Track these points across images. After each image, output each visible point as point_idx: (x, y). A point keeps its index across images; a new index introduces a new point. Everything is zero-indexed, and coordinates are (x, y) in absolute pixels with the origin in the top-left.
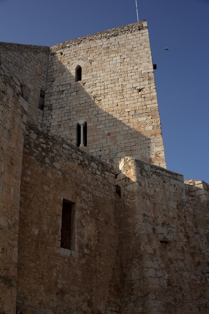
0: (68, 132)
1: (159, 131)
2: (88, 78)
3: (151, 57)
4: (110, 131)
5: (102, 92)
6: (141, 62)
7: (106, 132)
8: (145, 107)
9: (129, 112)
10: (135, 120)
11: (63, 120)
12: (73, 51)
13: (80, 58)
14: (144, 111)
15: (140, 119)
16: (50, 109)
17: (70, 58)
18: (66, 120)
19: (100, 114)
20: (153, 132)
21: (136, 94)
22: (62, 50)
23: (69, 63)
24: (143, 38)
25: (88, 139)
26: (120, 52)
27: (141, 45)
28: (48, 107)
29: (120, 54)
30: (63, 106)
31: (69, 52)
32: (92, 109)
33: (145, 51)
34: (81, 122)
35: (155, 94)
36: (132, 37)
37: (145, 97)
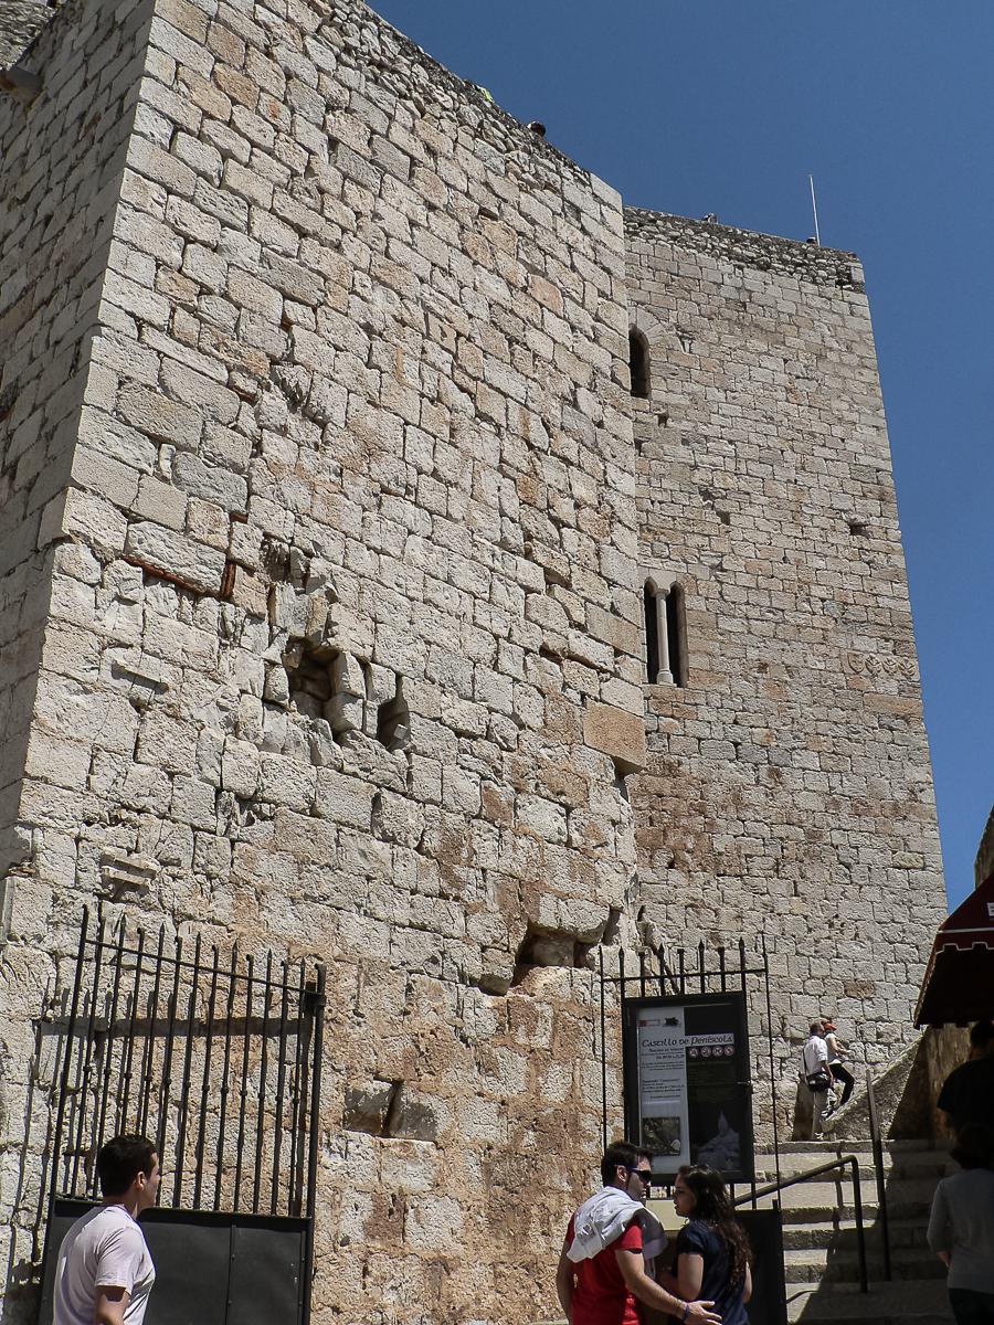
1: (915, 705)
2: (674, 399)
3: (882, 412)
4: (767, 657)
5: (731, 482)
6: (854, 417)
7: (753, 654)
8: (871, 602)
9: (823, 600)
13: (642, 299)
14: (872, 617)
15: (862, 644)
19: (726, 571)
20: (902, 705)
21: (842, 538)
24: (854, 323)
25: (694, 662)
26: (784, 343)
29: (782, 351)
32: (699, 540)
33: (862, 378)
34: (664, 583)
35: (899, 561)
36: (818, 302)
37: (872, 562)
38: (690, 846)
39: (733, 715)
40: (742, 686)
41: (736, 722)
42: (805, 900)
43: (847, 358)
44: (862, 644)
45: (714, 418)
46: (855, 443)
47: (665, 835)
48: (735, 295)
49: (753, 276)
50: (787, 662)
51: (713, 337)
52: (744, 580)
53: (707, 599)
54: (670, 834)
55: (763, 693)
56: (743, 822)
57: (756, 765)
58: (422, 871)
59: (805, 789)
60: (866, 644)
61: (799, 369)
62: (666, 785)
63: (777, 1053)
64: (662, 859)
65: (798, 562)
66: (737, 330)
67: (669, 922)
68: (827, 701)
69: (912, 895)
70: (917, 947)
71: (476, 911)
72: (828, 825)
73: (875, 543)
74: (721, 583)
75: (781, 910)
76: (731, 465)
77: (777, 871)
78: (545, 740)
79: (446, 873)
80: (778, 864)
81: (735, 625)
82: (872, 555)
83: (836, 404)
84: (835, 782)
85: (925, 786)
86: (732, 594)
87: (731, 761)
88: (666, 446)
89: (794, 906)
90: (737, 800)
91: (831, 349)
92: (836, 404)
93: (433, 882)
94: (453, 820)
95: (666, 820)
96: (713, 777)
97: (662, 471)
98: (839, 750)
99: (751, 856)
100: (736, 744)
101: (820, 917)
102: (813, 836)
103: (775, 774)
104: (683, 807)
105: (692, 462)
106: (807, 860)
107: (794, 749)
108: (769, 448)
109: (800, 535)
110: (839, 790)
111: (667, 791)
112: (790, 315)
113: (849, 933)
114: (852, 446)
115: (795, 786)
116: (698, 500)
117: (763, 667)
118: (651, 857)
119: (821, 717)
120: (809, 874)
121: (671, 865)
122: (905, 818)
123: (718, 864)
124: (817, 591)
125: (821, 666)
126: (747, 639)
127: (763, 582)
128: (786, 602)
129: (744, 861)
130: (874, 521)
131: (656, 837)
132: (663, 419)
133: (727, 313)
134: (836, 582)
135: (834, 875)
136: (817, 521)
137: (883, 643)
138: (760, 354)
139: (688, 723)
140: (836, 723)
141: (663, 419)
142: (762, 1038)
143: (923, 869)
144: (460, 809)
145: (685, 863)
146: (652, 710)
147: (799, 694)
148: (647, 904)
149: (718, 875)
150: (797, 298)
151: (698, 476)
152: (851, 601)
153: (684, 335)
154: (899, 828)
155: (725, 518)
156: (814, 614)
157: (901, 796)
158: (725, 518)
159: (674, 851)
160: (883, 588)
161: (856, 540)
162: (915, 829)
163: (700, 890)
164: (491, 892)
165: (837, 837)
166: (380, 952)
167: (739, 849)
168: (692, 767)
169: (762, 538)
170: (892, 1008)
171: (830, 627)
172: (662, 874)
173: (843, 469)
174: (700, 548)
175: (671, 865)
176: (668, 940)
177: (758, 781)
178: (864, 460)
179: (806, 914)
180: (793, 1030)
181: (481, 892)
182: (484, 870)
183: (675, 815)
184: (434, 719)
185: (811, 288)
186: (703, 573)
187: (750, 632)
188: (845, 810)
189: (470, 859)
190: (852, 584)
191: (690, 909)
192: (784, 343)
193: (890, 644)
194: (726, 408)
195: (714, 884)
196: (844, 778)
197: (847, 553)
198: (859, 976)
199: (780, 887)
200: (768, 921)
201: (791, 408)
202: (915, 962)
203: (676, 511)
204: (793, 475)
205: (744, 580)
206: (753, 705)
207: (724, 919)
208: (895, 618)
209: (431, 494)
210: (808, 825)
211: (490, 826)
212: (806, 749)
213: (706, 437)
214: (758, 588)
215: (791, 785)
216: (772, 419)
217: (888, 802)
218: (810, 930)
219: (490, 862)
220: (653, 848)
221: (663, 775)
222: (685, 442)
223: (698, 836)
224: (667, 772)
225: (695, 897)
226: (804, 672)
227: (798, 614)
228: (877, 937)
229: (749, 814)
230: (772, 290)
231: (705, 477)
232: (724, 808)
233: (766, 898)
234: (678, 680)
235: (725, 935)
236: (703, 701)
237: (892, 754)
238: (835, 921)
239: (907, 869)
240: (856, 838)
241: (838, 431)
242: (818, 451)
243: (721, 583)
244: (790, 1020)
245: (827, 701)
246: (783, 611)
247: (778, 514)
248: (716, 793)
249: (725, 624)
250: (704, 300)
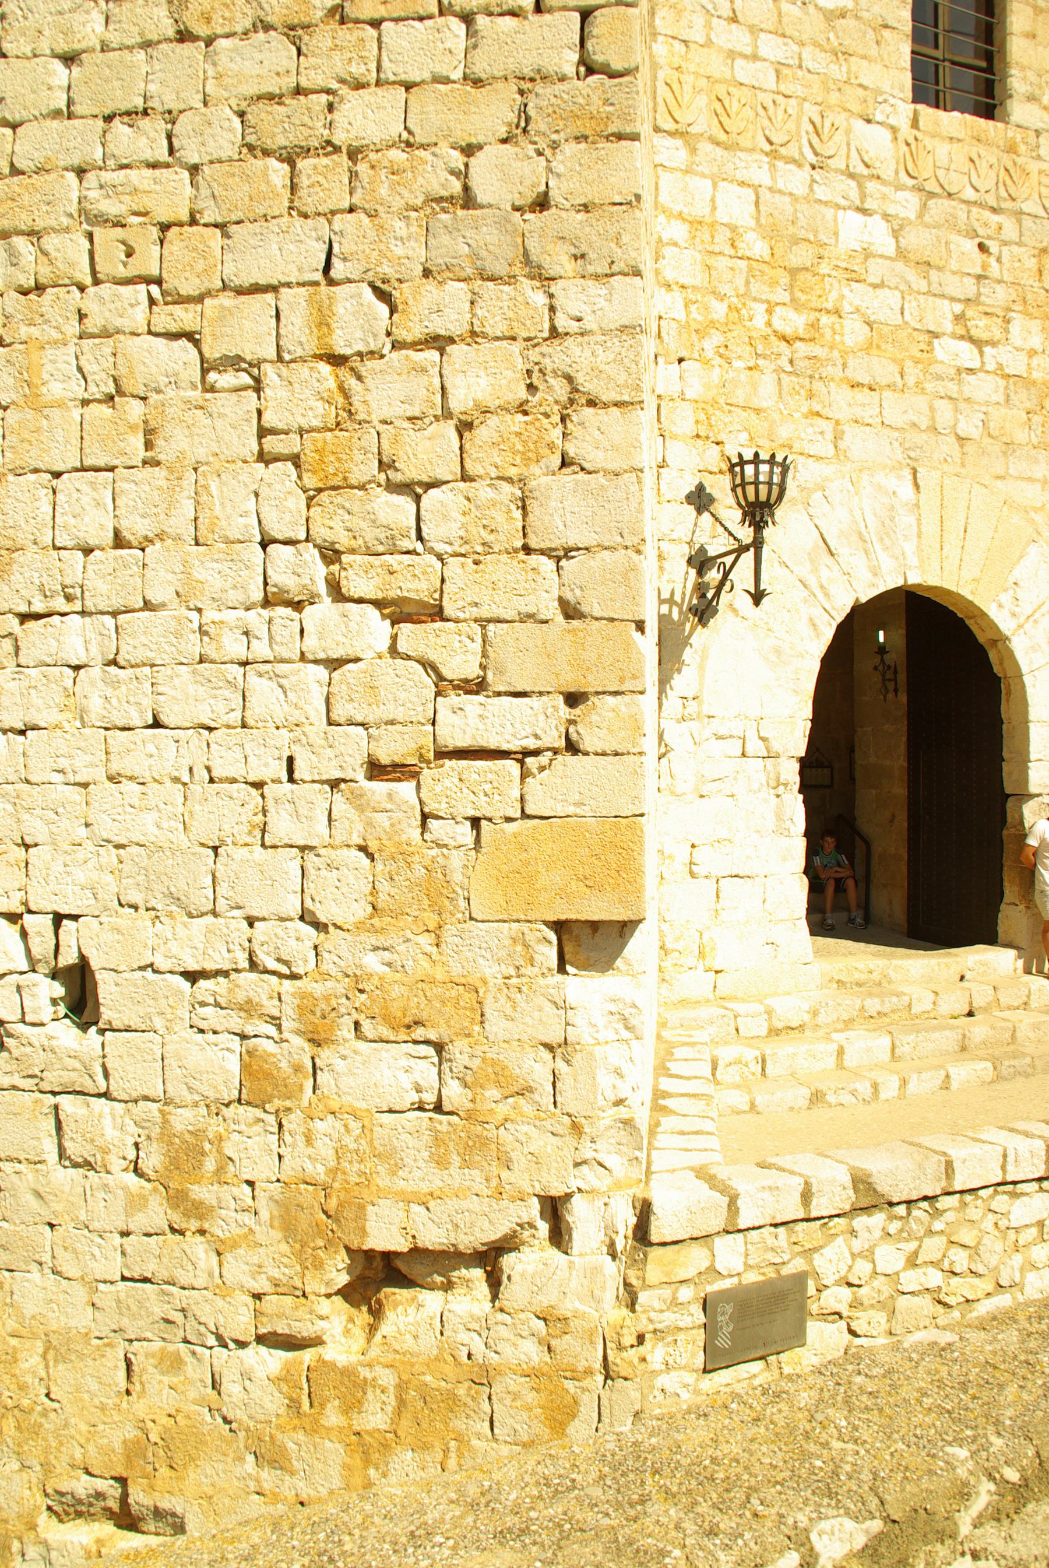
58: (135, 1203)
71: (235, 1245)
78: (373, 940)
79: (177, 1199)
93: (157, 1213)
94: (183, 1120)
144: (197, 1098)
164: (264, 1215)
166: (82, 1319)
181: (248, 1219)
182: (251, 1183)
184: (142, 968)
189: (220, 1170)
209: (105, 579)
211: (259, 1113)
219: (263, 1169)
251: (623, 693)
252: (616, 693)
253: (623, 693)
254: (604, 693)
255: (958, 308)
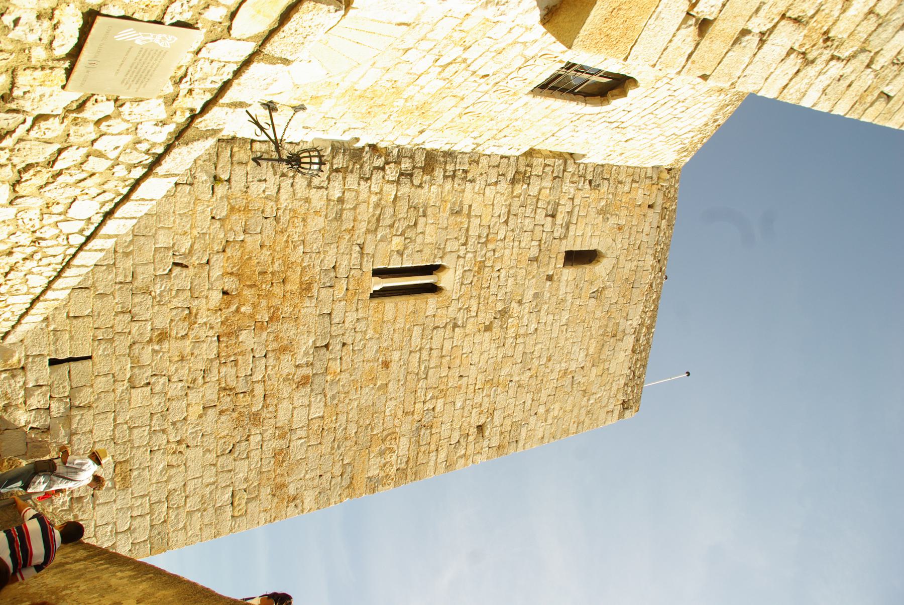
0: (428, 240)
4: (394, 367)
5: (511, 332)
6: (550, 421)
7: (396, 356)
8: (433, 447)
10: (406, 428)
11: (469, 222)
12: (645, 239)
14: (423, 449)
15: (404, 441)
16: (517, 177)
17: (630, 234)
18: (467, 230)
19: (453, 331)
21: (475, 420)
22: (658, 209)
23: (620, 228)
25: (389, 304)
26: (593, 365)
27: (588, 412)
28: (525, 172)
29: (589, 365)
30: (511, 217)
31: (647, 229)
32: (474, 308)
34: (444, 280)
36: (615, 387)
38: (243, 309)
39: (349, 341)
40: (372, 346)
41: (344, 344)
42: (200, 416)
43: (583, 411)
44: (404, 441)
45: (551, 317)
46: (534, 422)
47: (251, 286)
48: (621, 328)
49: (630, 341)
50: (390, 385)
51: (598, 314)
52: (448, 345)
53: (434, 316)
54: (253, 291)
55: (367, 366)
56: (265, 356)
57: (312, 364)
59: (294, 408)
60: (403, 446)
61: (579, 378)
62: (293, 286)
63: (54, 405)
64: (230, 284)
65: (460, 387)
66: (601, 332)
67: (174, 293)
68: (362, 419)
69: (211, 511)
70: (165, 521)
72: (266, 430)
73: (471, 447)
74: (444, 327)
75: (191, 396)
76: (522, 331)
77: (225, 389)
80: (231, 389)
81: (416, 341)
82: (464, 444)
83: (557, 406)
84: (300, 433)
85: (300, 508)
86: (438, 335)
87: (314, 342)
88: (534, 281)
89: (196, 407)
90: (284, 349)
91: (589, 400)
92: (557, 406)
95: (264, 286)
96: (301, 327)
97: (519, 278)
98: (325, 433)
99: (236, 365)
100: (327, 346)
101: (187, 431)
102: (256, 419)
103: (305, 381)
104: (276, 302)
105: (524, 301)
106: (235, 415)
107: (325, 396)
108: (532, 359)
109: (477, 387)
110: (294, 437)
111: (288, 287)
112: (608, 369)
113: (174, 459)
114: (533, 420)
115: (296, 399)
116: (500, 306)
117: (386, 365)
118: (232, 274)
119: (350, 416)
120: (223, 418)
121: (225, 293)
122: (274, 495)
123: (229, 335)
124: (440, 402)
125: (387, 413)
126: (406, 351)
127: (445, 361)
128: (432, 380)
129: (232, 358)
130: (486, 443)
131: (249, 278)
132: (550, 278)
133: (611, 325)
134: (446, 418)
135: (223, 440)
136: (486, 399)
137: (405, 460)
138: (588, 349)
139: (343, 303)
140: (345, 429)
141: (550, 278)
142: (68, 388)
143: (233, 516)
145: (228, 305)
146: (353, 272)
147: (367, 396)
148: (191, 271)
149: (218, 337)
150: (618, 373)
151: (514, 305)
152: (434, 431)
153: (597, 295)
154: (266, 492)
155: (488, 328)
156: (424, 402)
157: (292, 490)
158: (488, 328)
159: (238, 295)
160: (442, 455)
161: (473, 430)
162: (266, 504)
163: (205, 320)
165: (255, 439)
167: (242, 353)
168: (308, 308)
169: (475, 358)
170: (105, 509)
171: (415, 416)
172: (219, 285)
173: (518, 416)
174: (468, 309)
175: (225, 293)
176: (158, 292)
177: (297, 366)
178: (524, 431)
179: (189, 418)
180: (79, 417)
183: (269, 295)
185: (622, 382)
186: (452, 311)
187: (411, 352)
188: (282, 443)
190: (445, 430)
191: (187, 312)
192: (593, 365)
193: (403, 466)
194: (556, 326)
195: (211, 333)
196: (303, 441)
197: (465, 424)
198: (135, 473)
199: (211, 392)
200: (180, 384)
201: (554, 375)
202: (152, 520)
203: (493, 290)
204: (516, 379)
205: (448, 345)
206: (358, 359)
207: (180, 343)
208: (422, 467)
210: (264, 414)
212: (326, 405)
213: (539, 311)
214: (442, 357)
215: (296, 395)
216: (550, 360)
217: (288, 479)
218: (174, 424)
220: (239, 276)
221: (301, 283)
222: (536, 295)
223: (252, 316)
224: (304, 286)
225: (198, 316)
226: (383, 399)
227: (424, 390)
228: (171, 486)
229: (271, 361)
230: (622, 354)
231: (515, 311)
232: (276, 338)
233: (200, 381)
234: (376, 295)
235: (166, 345)
236: (360, 316)
237: (324, 477)
238: (184, 446)
239: (232, 504)
240: (256, 455)
241: (542, 410)
242: (530, 396)
243: (444, 327)
244: (89, 415)
245: (362, 419)
246: (426, 378)
247: (491, 369)
248: (288, 330)
249: (417, 331)
250: (619, 306)
251: (687, 60)
252: (690, 56)
253: (687, 60)
254: (695, 48)
255: (468, 62)
